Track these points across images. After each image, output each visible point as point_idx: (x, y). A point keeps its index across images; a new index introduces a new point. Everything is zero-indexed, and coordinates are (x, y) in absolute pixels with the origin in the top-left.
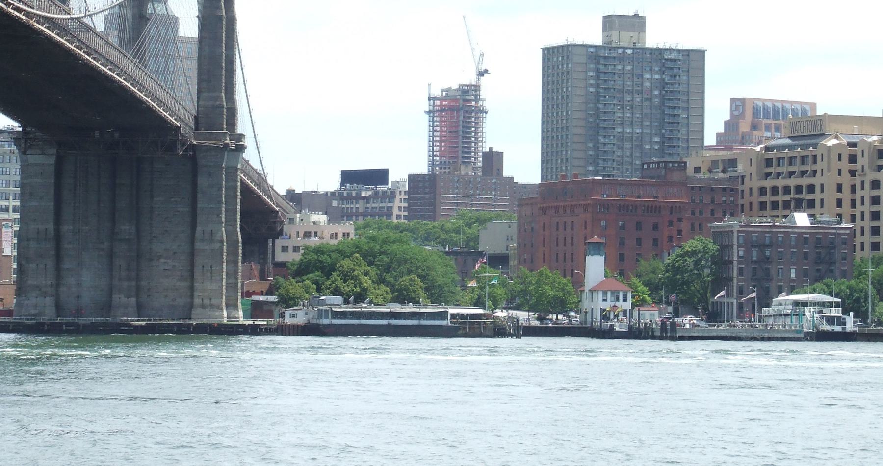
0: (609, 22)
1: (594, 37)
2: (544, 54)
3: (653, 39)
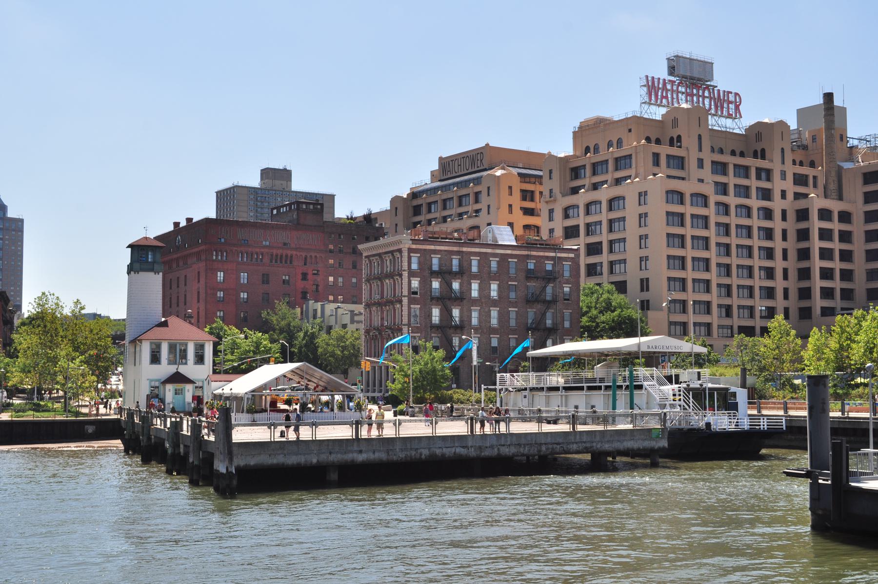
0: (266, 173)
1: (255, 181)
2: (217, 196)
3: (298, 185)
